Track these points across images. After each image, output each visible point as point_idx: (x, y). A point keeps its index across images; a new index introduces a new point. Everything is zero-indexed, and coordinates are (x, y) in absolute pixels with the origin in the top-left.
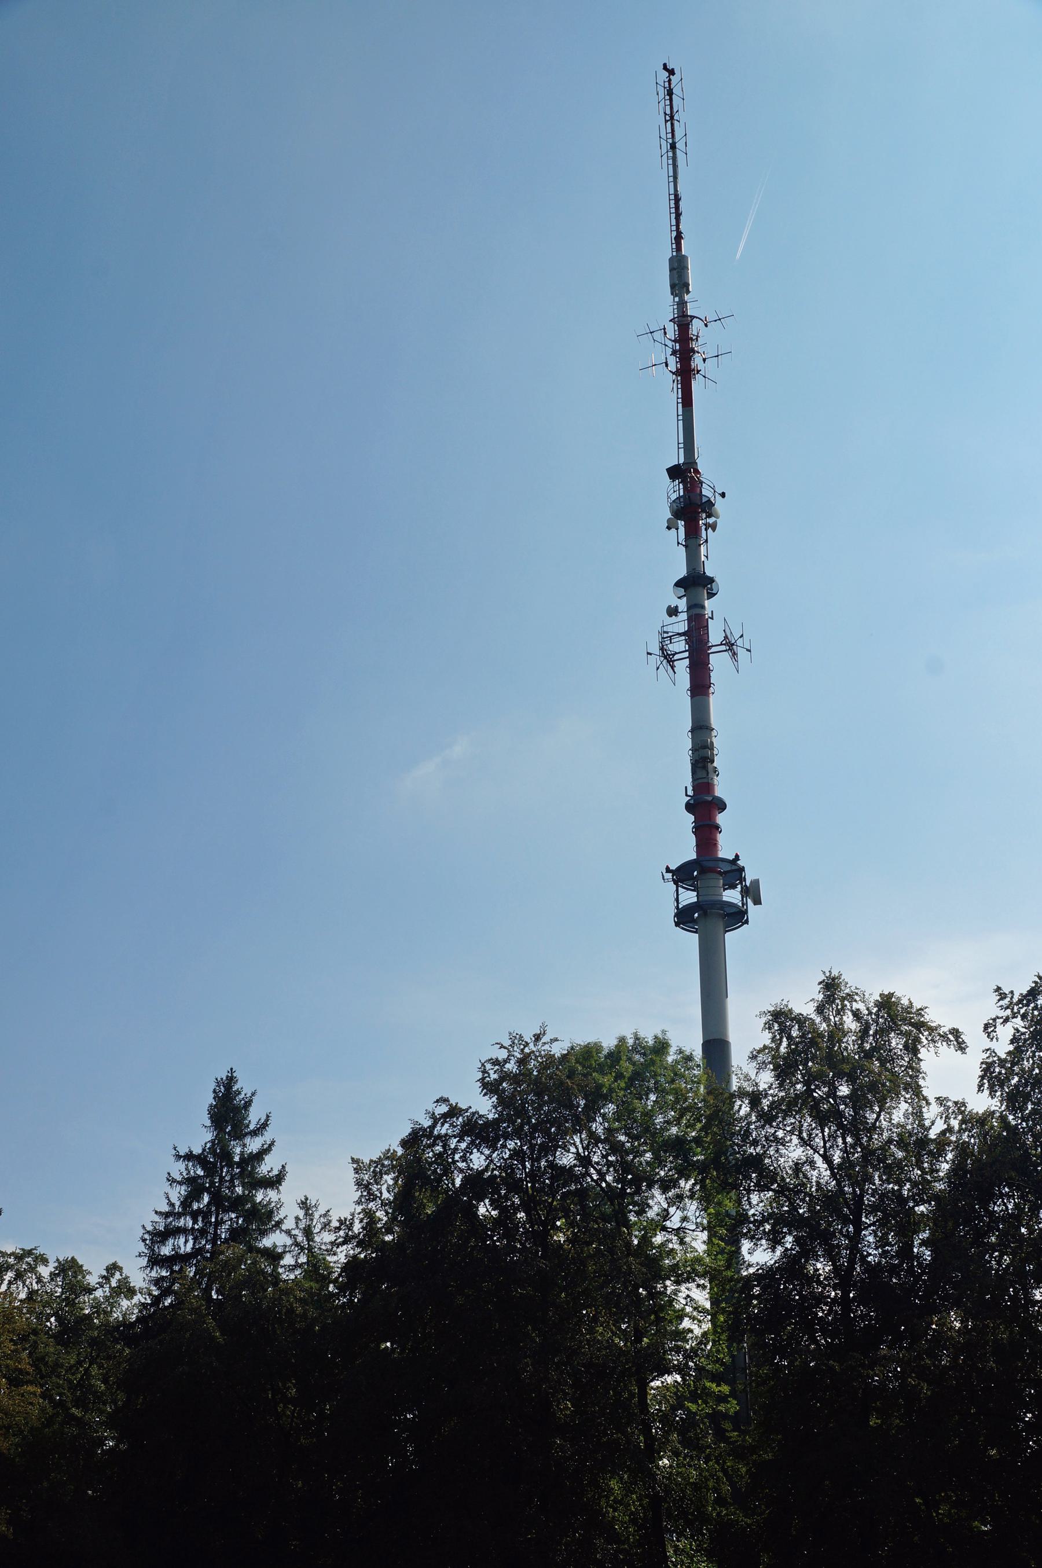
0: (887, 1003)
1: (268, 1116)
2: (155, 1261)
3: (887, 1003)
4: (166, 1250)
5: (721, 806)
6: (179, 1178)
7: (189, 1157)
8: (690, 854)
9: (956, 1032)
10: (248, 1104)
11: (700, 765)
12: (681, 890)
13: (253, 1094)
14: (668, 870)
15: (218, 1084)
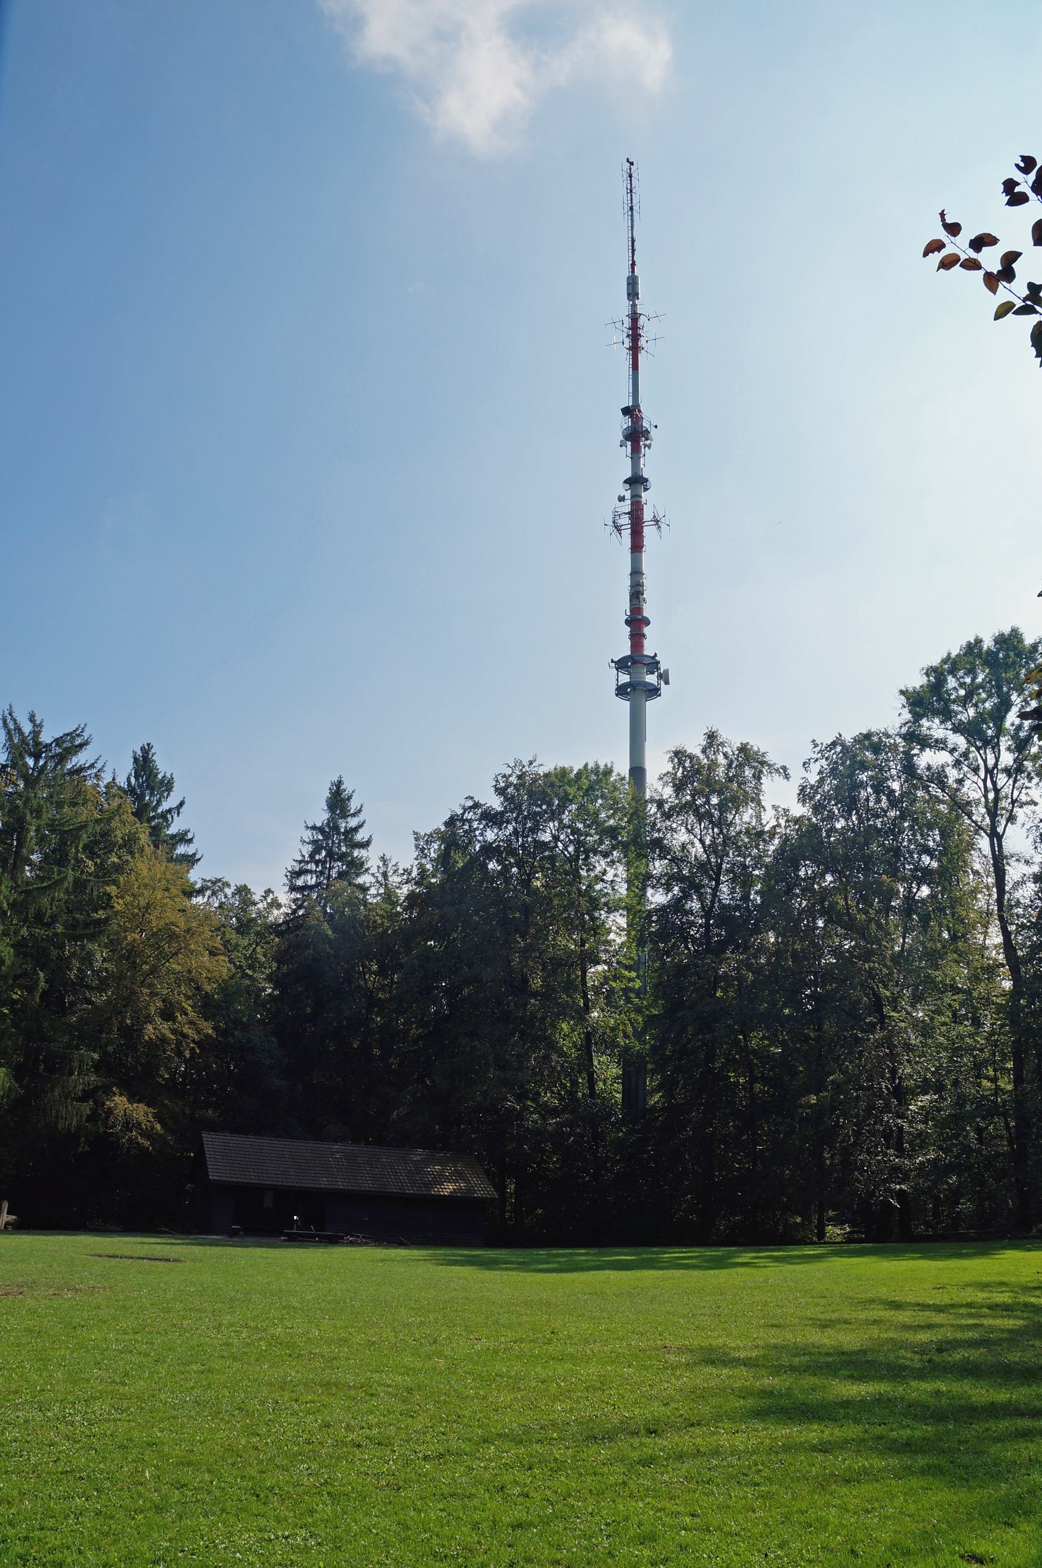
0: (744, 749)
2: (293, 888)
3: (744, 749)
4: (300, 882)
5: (647, 622)
7: (314, 828)
8: (628, 652)
9: (784, 768)
10: (349, 798)
14: (612, 661)
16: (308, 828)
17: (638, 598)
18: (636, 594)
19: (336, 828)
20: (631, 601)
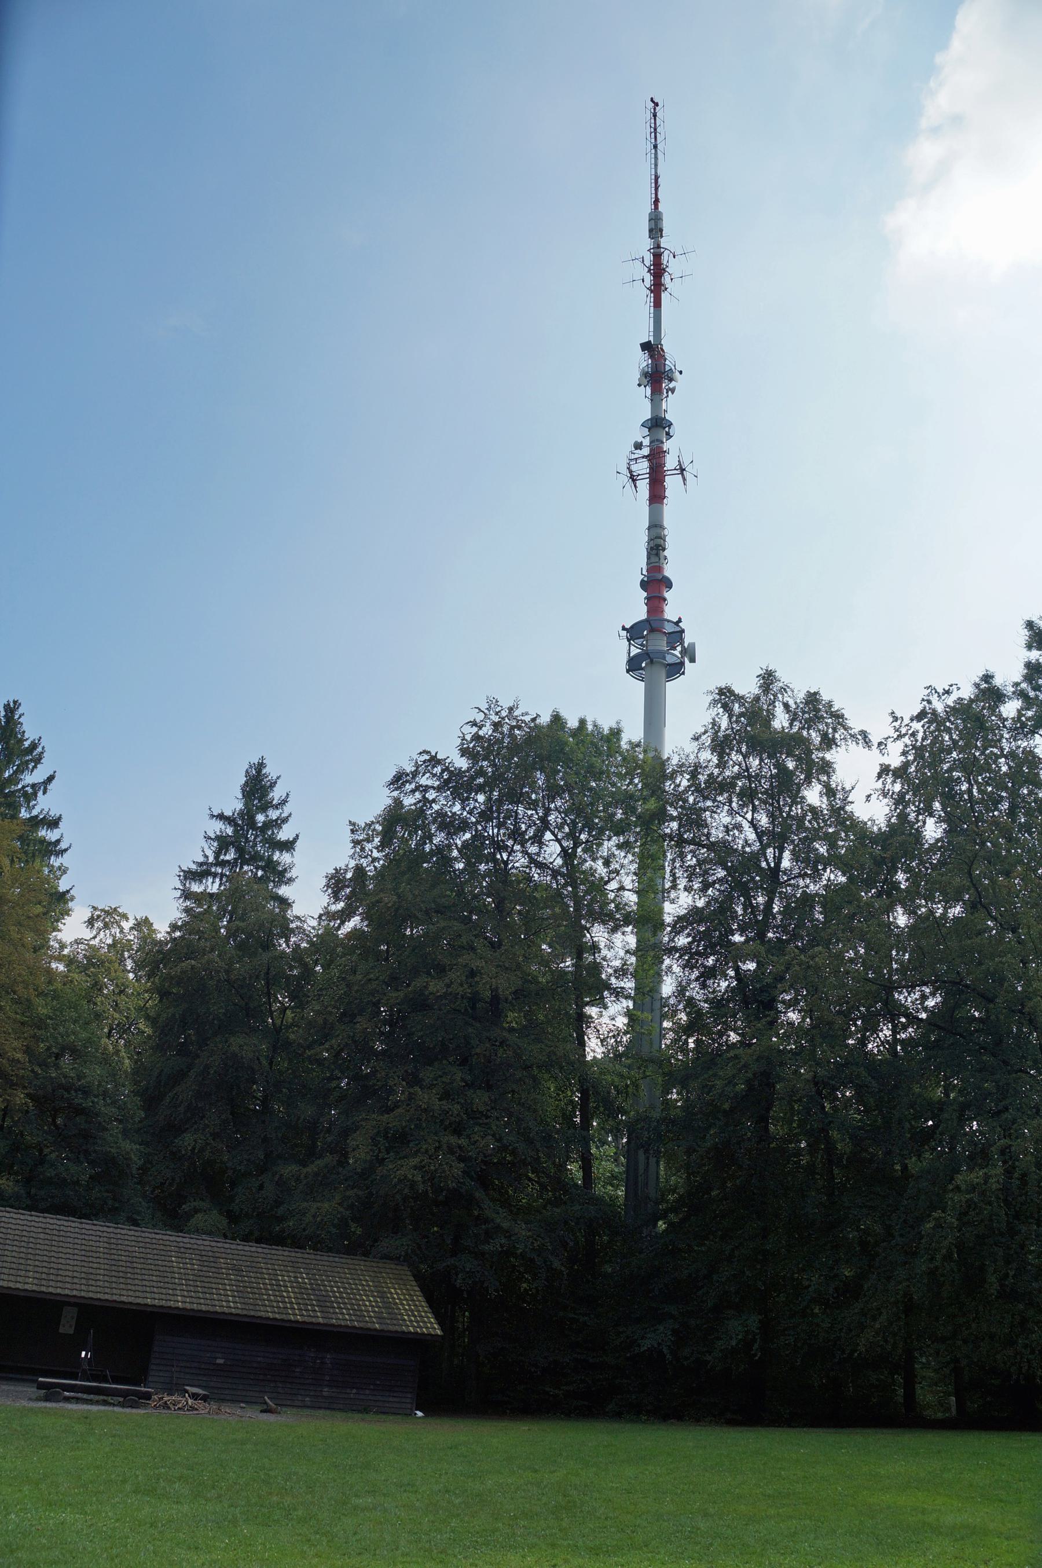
0: (813, 698)
1: (288, 794)
2: (187, 895)
3: (813, 698)
4: (196, 888)
5: (669, 585)
6: (213, 836)
7: (221, 817)
8: (641, 613)
9: (864, 734)
10: (273, 784)
11: (654, 552)
12: (632, 647)
13: (278, 778)
14: (624, 628)
15: (251, 767)
16: (213, 816)
17: (657, 555)
18: (656, 548)
19: (252, 823)
20: (648, 558)
